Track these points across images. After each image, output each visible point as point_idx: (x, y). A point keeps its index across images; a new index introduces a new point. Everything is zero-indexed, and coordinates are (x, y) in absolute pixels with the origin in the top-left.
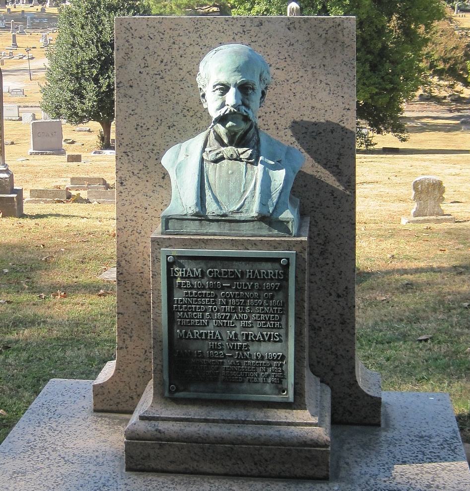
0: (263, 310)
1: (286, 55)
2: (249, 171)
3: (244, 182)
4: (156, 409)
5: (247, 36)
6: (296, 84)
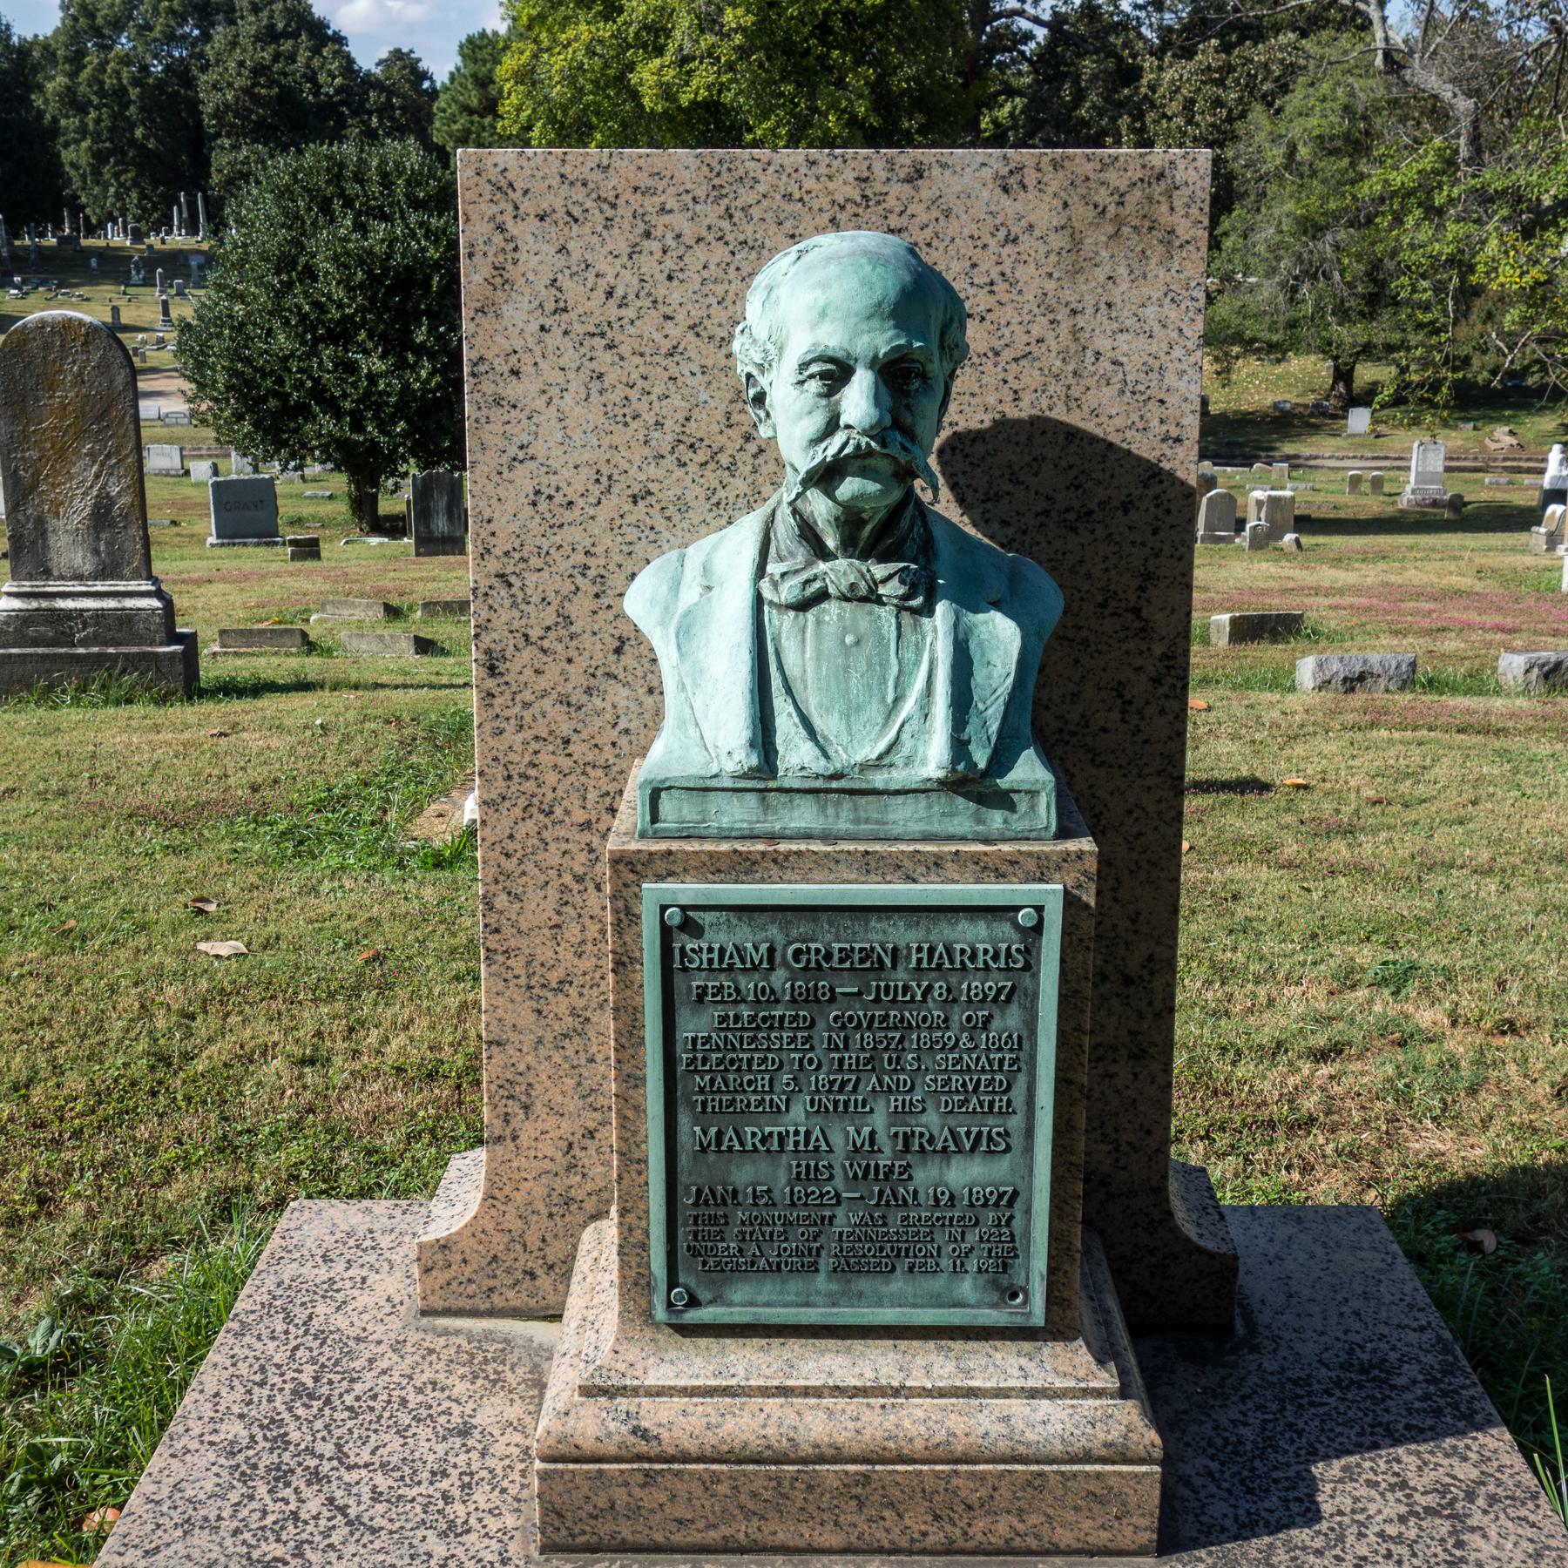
0: (959, 1060)
1: (995, 275)
2: (910, 637)
3: (894, 670)
4: (631, 1358)
5: (874, 214)
6: (1023, 362)
